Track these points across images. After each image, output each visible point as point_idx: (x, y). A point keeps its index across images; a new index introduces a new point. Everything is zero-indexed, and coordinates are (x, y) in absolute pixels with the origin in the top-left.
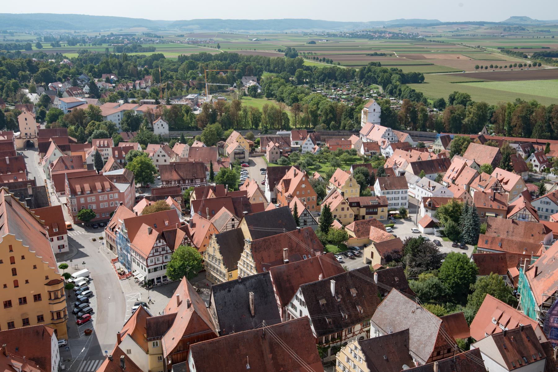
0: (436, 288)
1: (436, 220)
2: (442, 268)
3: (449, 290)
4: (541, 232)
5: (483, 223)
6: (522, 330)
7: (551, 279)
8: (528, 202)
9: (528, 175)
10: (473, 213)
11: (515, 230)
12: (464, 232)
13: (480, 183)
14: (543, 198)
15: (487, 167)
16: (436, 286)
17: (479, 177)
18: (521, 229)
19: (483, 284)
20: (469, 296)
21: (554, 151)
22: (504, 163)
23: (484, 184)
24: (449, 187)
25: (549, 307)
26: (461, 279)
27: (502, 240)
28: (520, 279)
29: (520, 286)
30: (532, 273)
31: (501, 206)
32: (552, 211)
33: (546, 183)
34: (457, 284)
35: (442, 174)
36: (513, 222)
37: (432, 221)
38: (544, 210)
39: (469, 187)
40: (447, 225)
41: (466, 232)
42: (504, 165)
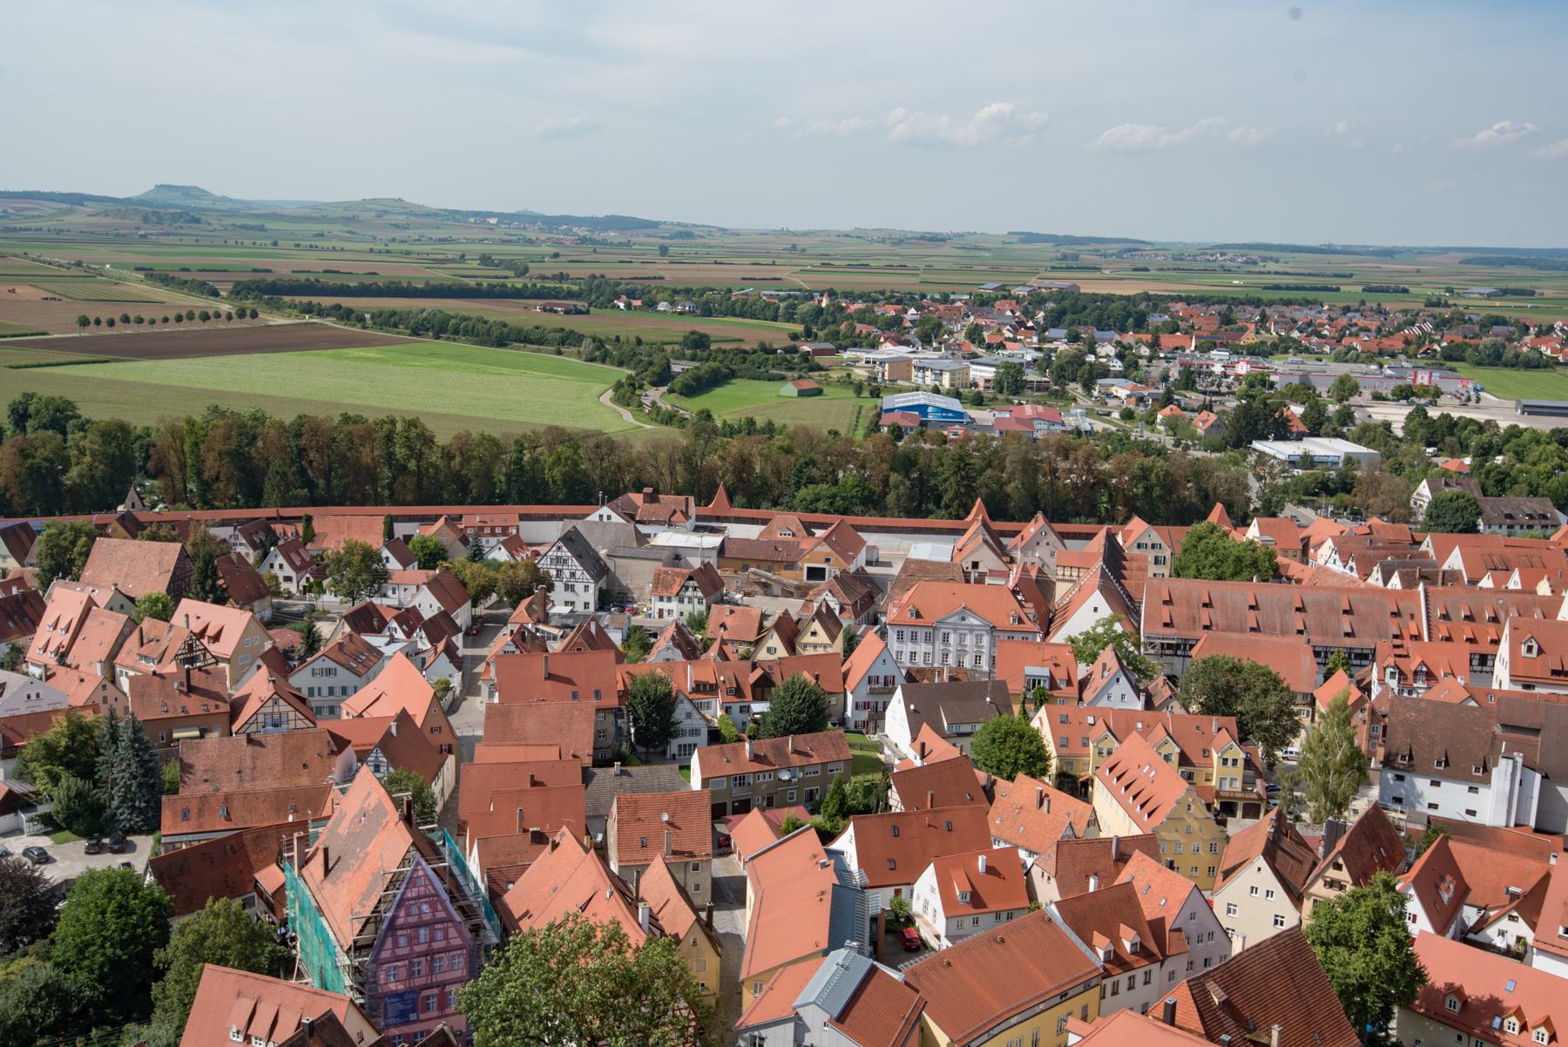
0: (50, 995)
1: (20, 788)
2: (62, 929)
3: (94, 988)
4: (326, 752)
5: (167, 762)
6: (311, 1035)
7: (365, 869)
8: (280, 680)
9: (272, 606)
10: (133, 741)
11: (259, 763)
12: (115, 803)
13: (143, 651)
14: (319, 662)
15: (158, 600)
16: (51, 992)
17: (136, 634)
18: (272, 756)
19: (190, 938)
20: (156, 989)
21: (325, 535)
22: (202, 584)
23: (154, 650)
24: (48, 678)
25: (370, 946)
26: (123, 945)
27: (228, 798)
28: (289, 894)
29: (291, 911)
30: (317, 866)
31: (212, 703)
32: (344, 691)
33: (318, 619)
34: (114, 963)
35: (21, 641)
36: (250, 741)
37: (10, 793)
38: (325, 692)
39: (113, 668)
40: (59, 792)
41: (123, 802)
42: (203, 588)
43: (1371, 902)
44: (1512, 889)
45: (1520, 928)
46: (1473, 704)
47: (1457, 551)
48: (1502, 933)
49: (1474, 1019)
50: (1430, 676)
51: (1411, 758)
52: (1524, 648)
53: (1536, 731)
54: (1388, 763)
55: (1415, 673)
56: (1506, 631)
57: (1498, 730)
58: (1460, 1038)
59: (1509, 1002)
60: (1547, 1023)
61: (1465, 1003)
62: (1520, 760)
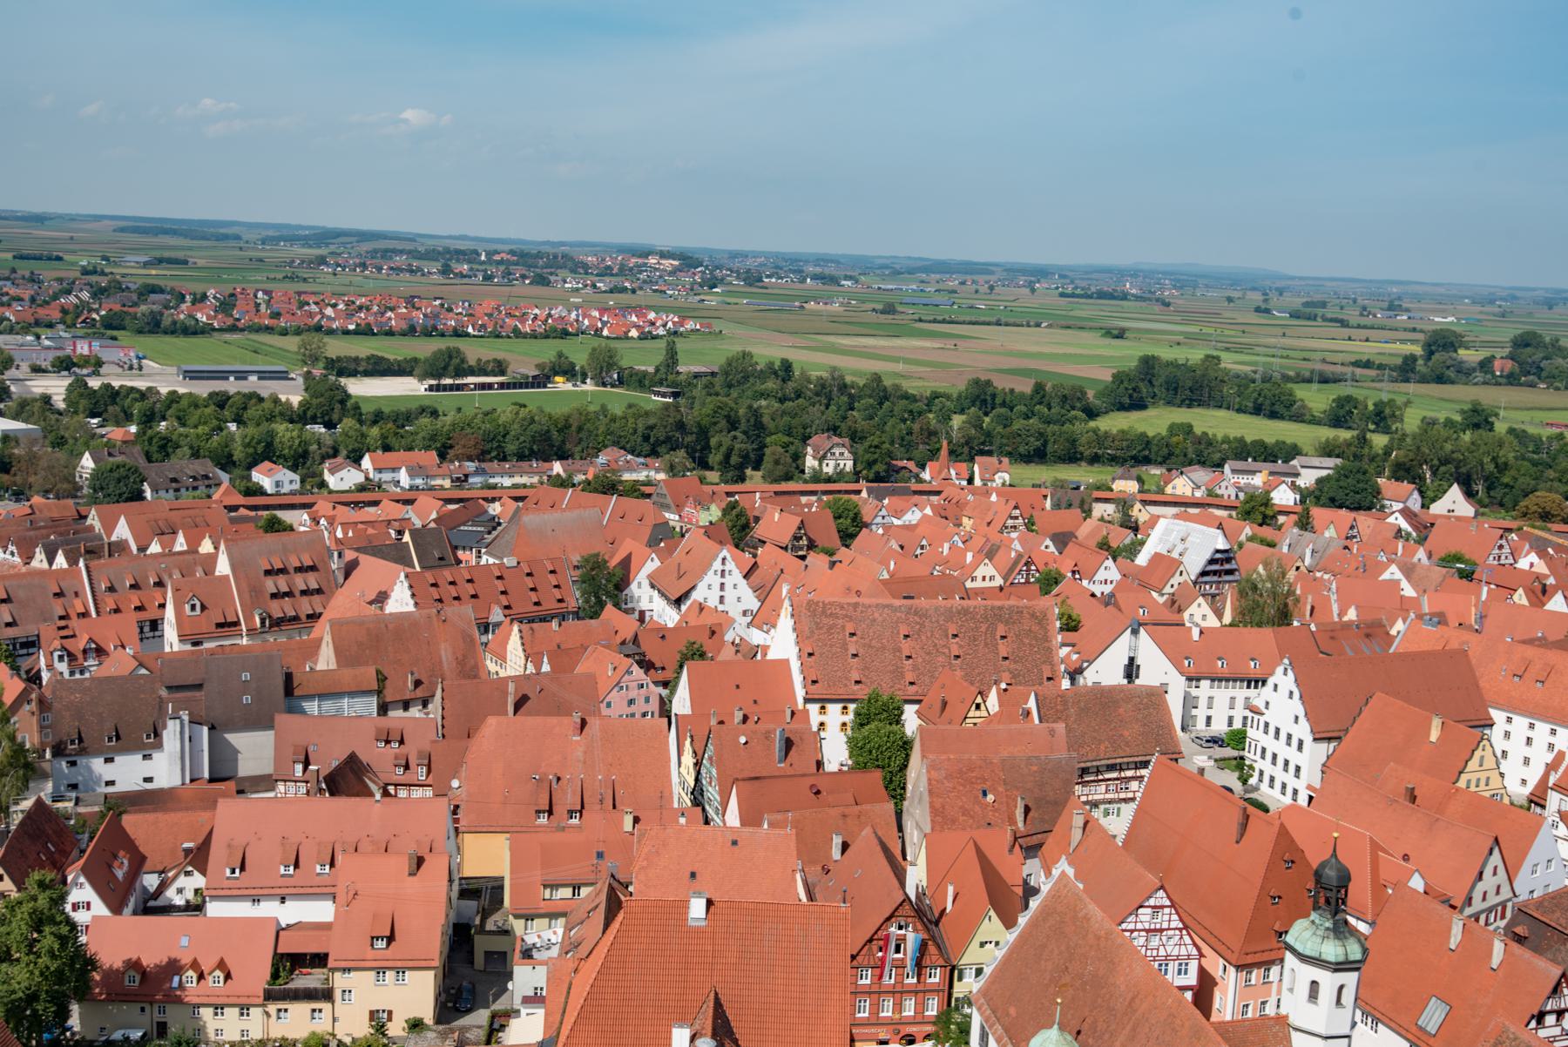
43: (27, 907)
44: (186, 845)
45: (198, 880)
46: (143, 671)
47: (122, 520)
48: (180, 891)
49: (151, 986)
50: (100, 652)
51: (81, 740)
52: (187, 607)
53: (199, 687)
54: (58, 751)
55: (85, 651)
56: (169, 594)
57: (164, 693)
58: (143, 1010)
59: (186, 960)
60: (221, 965)
61: (144, 974)
62: (186, 718)
